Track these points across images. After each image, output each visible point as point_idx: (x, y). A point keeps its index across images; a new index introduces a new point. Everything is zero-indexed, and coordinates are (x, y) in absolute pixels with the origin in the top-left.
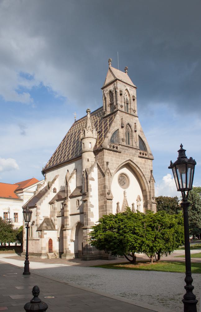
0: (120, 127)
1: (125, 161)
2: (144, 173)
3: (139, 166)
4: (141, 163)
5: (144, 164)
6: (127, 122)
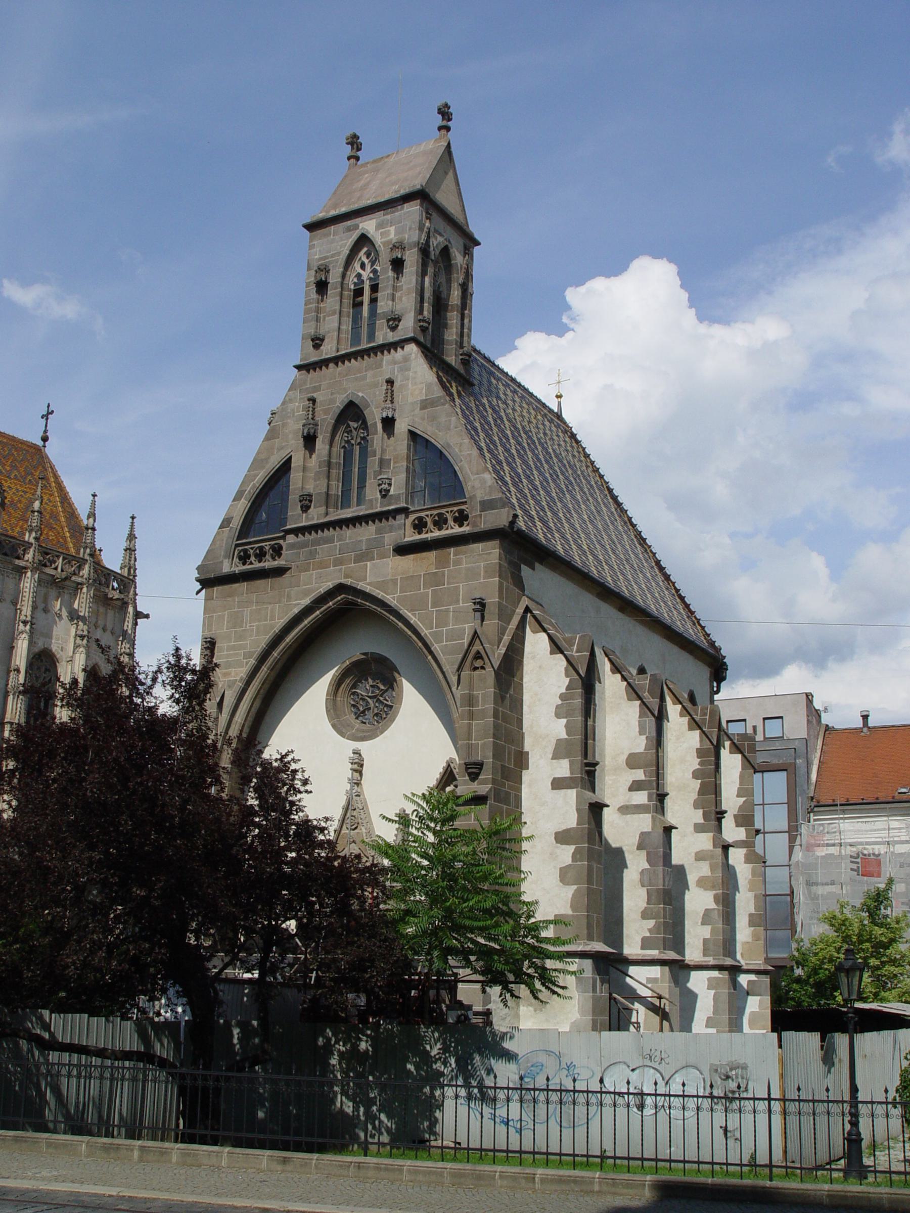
0: (294, 446)
1: (306, 601)
2: (425, 632)
3: (391, 599)
4: (410, 580)
5: (435, 580)
6: (339, 402)
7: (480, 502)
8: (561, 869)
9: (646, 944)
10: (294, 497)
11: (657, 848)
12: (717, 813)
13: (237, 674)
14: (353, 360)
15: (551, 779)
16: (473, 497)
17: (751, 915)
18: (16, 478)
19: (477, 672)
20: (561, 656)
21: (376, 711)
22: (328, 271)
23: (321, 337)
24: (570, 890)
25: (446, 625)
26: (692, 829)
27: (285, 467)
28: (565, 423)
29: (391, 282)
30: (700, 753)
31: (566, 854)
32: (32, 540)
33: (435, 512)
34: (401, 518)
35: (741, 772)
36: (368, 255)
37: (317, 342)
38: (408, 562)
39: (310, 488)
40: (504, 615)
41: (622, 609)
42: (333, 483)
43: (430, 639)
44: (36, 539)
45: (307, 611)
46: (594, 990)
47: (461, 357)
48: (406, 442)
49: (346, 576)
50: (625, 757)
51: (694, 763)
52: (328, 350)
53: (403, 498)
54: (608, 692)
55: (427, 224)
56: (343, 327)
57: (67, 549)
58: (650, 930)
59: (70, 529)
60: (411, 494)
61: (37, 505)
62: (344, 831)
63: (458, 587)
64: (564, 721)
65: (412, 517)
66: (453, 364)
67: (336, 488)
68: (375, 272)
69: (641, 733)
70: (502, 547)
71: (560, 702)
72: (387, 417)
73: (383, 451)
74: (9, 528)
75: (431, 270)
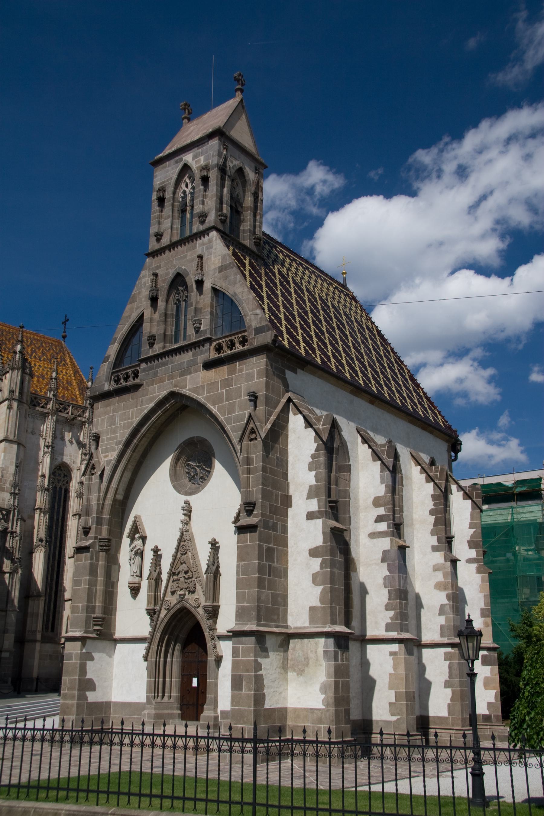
1: (152, 405)
2: (221, 418)
3: (202, 399)
4: (212, 385)
7: (254, 329)
8: (313, 575)
9: (389, 628)
10: (145, 338)
11: (394, 561)
12: (447, 538)
13: (112, 456)
14: (179, 247)
15: (306, 513)
16: (250, 326)
17: (482, 609)
18: (45, 360)
19: (252, 442)
20: (310, 429)
21: (201, 475)
22: (165, 191)
23: (160, 233)
24: (319, 589)
25: (234, 412)
26: (430, 549)
27: (141, 319)
28: (348, 290)
29: (202, 193)
30: (434, 497)
31: (316, 564)
32: (51, 396)
33: (228, 339)
34: (207, 346)
35: (471, 512)
36: (190, 178)
37: (159, 236)
38: (212, 374)
39: (154, 331)
40: (270, 403)
41: (371, 402)
42: (169, 327)
43: (224, 422)
44: (54, 395)
45: (152, 411)
46: (336, 659)
47: (253, 241)
48: (210, 295)
49: (175, 386)
50: (371, 500)
51: (430, 505)
52: (165, 241)
53: (209, 331)
54: (360, 457)
55: (225, 152)
56: (175, 226)
57: (77, 401)
58: (391, 618)
59: (79, 390)
60: (214, 328)
61: (54, 375)
62: (179, 555)
63: (241, 387)
64: (314, 473)
65: (214, 344)
66: (248, 245)
67: (171, 330)
68: (193, 188)
69: (382, 483)
70: (268, 357)
71: (311, 460)
72: (198, 280)
73: (197, 303)
74: (39, 390)
75: (227, 183)
